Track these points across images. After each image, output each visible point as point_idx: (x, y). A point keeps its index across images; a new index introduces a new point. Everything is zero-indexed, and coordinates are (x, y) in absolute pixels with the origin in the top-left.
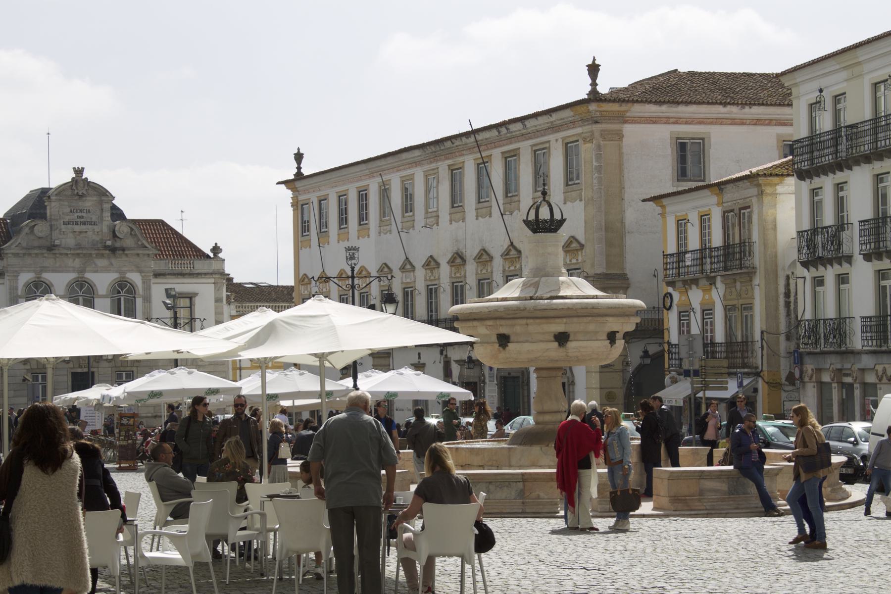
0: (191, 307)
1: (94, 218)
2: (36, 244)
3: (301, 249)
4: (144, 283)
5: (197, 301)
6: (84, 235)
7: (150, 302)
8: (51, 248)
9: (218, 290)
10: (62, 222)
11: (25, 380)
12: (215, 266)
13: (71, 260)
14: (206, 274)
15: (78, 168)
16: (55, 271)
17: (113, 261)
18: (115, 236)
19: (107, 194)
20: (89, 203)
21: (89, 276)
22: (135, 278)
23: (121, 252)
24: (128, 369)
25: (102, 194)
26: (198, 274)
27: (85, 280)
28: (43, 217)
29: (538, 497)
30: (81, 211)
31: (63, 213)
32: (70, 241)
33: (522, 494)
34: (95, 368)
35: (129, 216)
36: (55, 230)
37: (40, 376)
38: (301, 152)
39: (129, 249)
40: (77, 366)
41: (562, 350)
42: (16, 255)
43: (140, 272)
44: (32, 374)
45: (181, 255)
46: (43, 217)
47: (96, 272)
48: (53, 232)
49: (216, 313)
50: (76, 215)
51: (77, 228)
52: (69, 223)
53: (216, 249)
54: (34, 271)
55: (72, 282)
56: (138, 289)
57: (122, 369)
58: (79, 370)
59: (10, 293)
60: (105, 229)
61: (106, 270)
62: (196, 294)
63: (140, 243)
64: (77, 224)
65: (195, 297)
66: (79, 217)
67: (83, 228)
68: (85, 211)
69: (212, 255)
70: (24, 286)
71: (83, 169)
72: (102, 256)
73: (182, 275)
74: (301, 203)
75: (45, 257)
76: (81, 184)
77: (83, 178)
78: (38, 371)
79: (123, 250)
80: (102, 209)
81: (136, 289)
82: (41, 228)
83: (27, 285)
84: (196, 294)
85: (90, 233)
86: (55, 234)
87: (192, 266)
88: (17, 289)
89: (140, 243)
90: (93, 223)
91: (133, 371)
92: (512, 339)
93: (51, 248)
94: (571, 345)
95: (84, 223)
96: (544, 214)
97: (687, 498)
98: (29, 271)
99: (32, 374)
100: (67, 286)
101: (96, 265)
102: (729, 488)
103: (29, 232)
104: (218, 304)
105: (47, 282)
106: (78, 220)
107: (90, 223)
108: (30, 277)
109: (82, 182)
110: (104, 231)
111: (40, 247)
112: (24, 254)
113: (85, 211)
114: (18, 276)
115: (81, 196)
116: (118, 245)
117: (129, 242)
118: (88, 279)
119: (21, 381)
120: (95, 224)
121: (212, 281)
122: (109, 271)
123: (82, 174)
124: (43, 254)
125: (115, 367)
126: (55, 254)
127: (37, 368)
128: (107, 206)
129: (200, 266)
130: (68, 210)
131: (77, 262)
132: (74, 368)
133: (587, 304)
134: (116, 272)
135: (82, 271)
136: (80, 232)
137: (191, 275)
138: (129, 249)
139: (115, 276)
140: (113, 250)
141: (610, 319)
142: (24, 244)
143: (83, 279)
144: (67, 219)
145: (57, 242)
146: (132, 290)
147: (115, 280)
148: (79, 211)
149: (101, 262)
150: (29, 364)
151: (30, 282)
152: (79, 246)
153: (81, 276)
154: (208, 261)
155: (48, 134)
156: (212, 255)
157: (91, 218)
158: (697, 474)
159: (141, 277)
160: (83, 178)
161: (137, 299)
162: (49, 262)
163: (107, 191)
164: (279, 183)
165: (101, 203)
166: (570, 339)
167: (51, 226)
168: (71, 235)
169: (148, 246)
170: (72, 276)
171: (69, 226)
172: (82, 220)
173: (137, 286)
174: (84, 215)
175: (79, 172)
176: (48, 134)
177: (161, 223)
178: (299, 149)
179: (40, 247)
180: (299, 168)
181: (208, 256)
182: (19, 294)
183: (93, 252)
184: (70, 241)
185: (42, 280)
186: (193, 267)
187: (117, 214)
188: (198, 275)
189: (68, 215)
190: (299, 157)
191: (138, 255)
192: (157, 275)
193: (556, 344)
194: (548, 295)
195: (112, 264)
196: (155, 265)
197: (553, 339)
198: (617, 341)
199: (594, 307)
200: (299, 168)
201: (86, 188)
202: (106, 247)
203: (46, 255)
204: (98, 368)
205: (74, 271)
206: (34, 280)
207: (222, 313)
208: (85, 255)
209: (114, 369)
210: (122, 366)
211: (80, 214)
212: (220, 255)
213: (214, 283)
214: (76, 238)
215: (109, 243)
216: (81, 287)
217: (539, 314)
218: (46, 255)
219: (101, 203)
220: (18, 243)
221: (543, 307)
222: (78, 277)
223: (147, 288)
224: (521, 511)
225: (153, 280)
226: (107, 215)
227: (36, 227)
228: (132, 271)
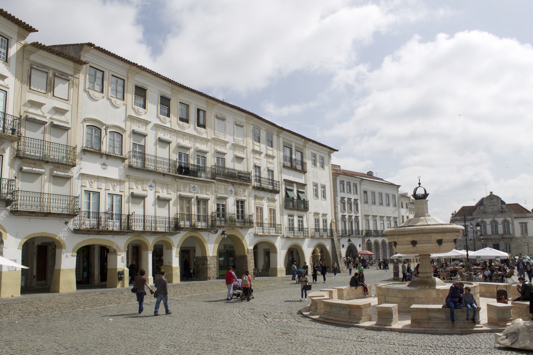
1: (496, 204)
2: (481, 212)
4: (511, 220)
5: (528, 224)
8: (485, 213)
11: (480, 246)
14: (530, 217)
18: (502, 208)
20: (495, 200)
21: (496, 219)
22: (509, 219)
25: (498, 198)
28: (483, 205)
29: (355, 315)
32: (490, 210)
33: (350, 313)
35: (507, 203)
39: (507, 211)
41: (414, 248)
43: (510, 217)
45: (523, 212)
46: (483, 205)
47: (498, 218)
51: (492, 207)
52: (489, 206)
60: (499, 207)
61: (500, 217)
62: (527, 223)
67: (494, 207)
72: (499, 214)
73: (523, 217)
76: (492, 196)
79: (505, 212)
82: (482, 208)
84: (527, 223)
86: (486, 209)
92: (398, 243)
93: (485, 213)
94: (418, 246)
95: (494, 206)
96: (420, 192)
97: (420, 321)
102: (446, 317)
107: (495, 206)
111: (482, 212)
115: (492, 199)
116: (503, 210)
117: (506, 210)
120: (496, 206)
128: (499, 201)
129: (528, 215)
130: (489, 203)
131: (492, 216)
133: (420, 228)
135: (494, 218)
137: (526, 217)
138: (507, 211)
139: (504, 219)
140: (502, 212)
141: (433, 234)
144: (489, 205)
145: (486, 211)
146: (508, 222)
149: (499, 215)
152: (493, 212)
154: (530, 214)
158: (425, 310)
165: (498, 200)
166: (418, 243)
167: (485, 207)
170: (492, 219)
175: (491, 193)
177: (517, 204)
179: (482, 212)
181: (531, 212)
183: (497, 213)
184: (490, 210)
187: (503, 203)
188: (528, 217)
192: (515, 218)
193: (411, 245)
194: (407, 225)
196: (514, 215)
197: (410, 243)
198: (443, 244)
199: (447, 229)
202: (500, 212)
208: (494, 214)
215: (501, 210)
216: (505, 221)
217: (402, 233)
219: (498, 200)
221: (402, 230)
223: (513, 222)
224: (346, 321)
225: (514, 219)
226: (500, 203)
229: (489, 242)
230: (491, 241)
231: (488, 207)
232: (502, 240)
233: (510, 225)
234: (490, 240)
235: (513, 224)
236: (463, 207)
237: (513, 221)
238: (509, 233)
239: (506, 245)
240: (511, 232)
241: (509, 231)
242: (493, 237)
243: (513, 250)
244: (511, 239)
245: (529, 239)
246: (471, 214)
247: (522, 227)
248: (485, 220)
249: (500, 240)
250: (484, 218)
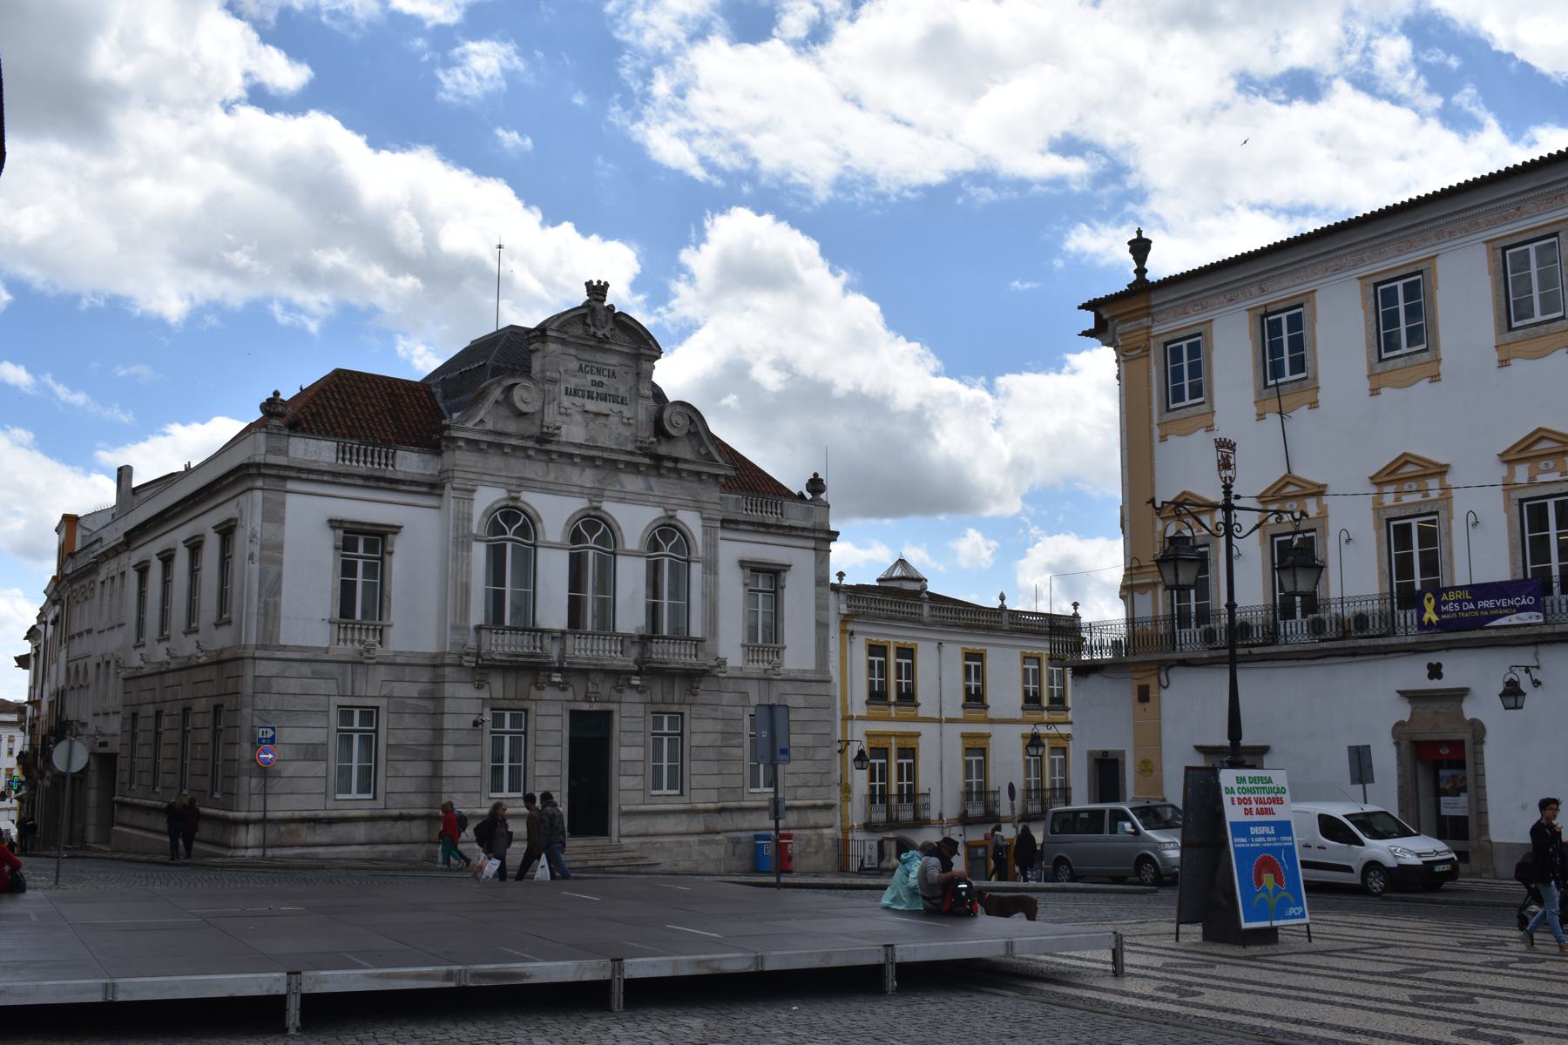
0: (775, 592)
1: (622, 391)
3: (1163, 438)
4: (705, 533)
6: (602, 420)
7: (716, 573)
9: (822, 562)
10: (563, 388)
12: (817, 518)
13: (577, 471)
15: (599, 282)
16: (546, 489)
17: (654, 481)
19: (651, 342)
22: (690, 520)
23: (670, 464)
24: (675, 708)
26: (791, 528)
27: (602, 515)
30: (599, 372)
31: (565, 371)
34: (614, 702)
36: (549, 404)
37: (507, 716)
38: (1144, 235)
40: (582, 697)
42: (473, 444)
43: (699, 509)
44: (492, 709)
47: (622, 500)
48: (546, 407)
49: (818, 607)
50: (590, 377)
51: (591, 405)
53: (816, 485)
54: (505, 485)
55: (578, 517)
56: (695, 543)
57: (663, 708)
58: (585, 707)
59: (456, 527)
60: (642, 415)
63: (703, 451)
64: (590, 397)
65: (785, 571)
66: (594, 383)
67: (603, 407)
68: (606, 373)
69: (808, 496)
70: (484, 514)
71: (607, 285)
74: (1167, 338)
75: (529, 457)
76: (601, 316)
77: (606, 304)
78: (505, 704)
80: (638, 374)
81: (692, 543)
82: (525, 397)
83: (490, 513)
85: (614, 419)
87: (779, 511)
88: (470, 520)
89: (703, 451)
90: (620, 400)
91: (682, 714)
95: (604, 398)
98: (495, 484)
99: (492, 709)
100: (567, 524)
101: (622, 486)
103: (501, 398)
104: (820, 589)
105: (530, 511)
106: (593, 389)
107: (616, 399)
108: (498, 497)
109: (603, 312)
110: (640, 418)
112: (490, 444)
113: (606, 373)
114: (473, 491)
116: (663, 450)
118: (606, 513)
119: (470, 725)
120: (623, 402)
121: (812, 544)
122: (644, 503)
123: (605, 296)
124: (525, 449)
125: (652, 702)
126: (549, 452)
127: (504, 699)
131: (588, 478)
132: (575, 701)
134: (658, 505)
135: (597, 494)
136: (597, 414)
142: (489, 426)
143: (598, 513)
144: (573, 382)
147: (655, 520)
148: (595, 371)
149: (633, 483)
150: (487, 686)
151: (496, 506)
153: (595, 504)
155: (500, 247)
156: (808, 496)
157: (617, 389)
159: (700, 522)
160: (606, 304)
161: (692, 564)
162: (535, 470)
163: (651, 337)
164: (1080, 308)
168: (578, 418)
169: (717, 457)
170: (577, 504)
171: (578, 401)
172: (601, 390)
173: (693, 538)
174: (605, 380)
176: (500, 247)
178: (1139, 232)
180: (1141, 271)
181: (801, 496)
182: (475, 531)
184: (574, 432)
185: (520, 505)
186: (781, 514)
189: (574, 376)
190: (1140, 248)
191: (699, 474)
192: (727, 523)
195: (650, 488)
200: (1141, 271)
201: (611, 325)
203: (531, 453)
204: (620, 702)
205: (581, 495)
206: (504, 503)
207: (827, 609)
209: (651, 708)
210: (663, 703)
211: (597, 378)
212: (823, 496)
213: (815, 549)
214: (587, 425)
218: (531, 453)
220: (478, 419)
222: (588, 509)
223: (712, 546)
225: (720, 534)
227: (517, 395)
228: (685, 507)
229: (549, 693)
230: (562, 687)
231: (567, 401)
232: (636, 681)
233: (696, 569)
234: (557, 678)
235: (711, 567)
236: (339, 373)
237: (715, 546)
238: (680, 635)
239: (658, 723)
240: (696, 631)
241: (681, 613)
242: (581, 650)
243: (696, 767)
244: (693, 677)
245: (788, 687)
246: (432, 439)
247: (752, 592)
248: (531, 499)
249: (618, 676)
250: (526, 483)
